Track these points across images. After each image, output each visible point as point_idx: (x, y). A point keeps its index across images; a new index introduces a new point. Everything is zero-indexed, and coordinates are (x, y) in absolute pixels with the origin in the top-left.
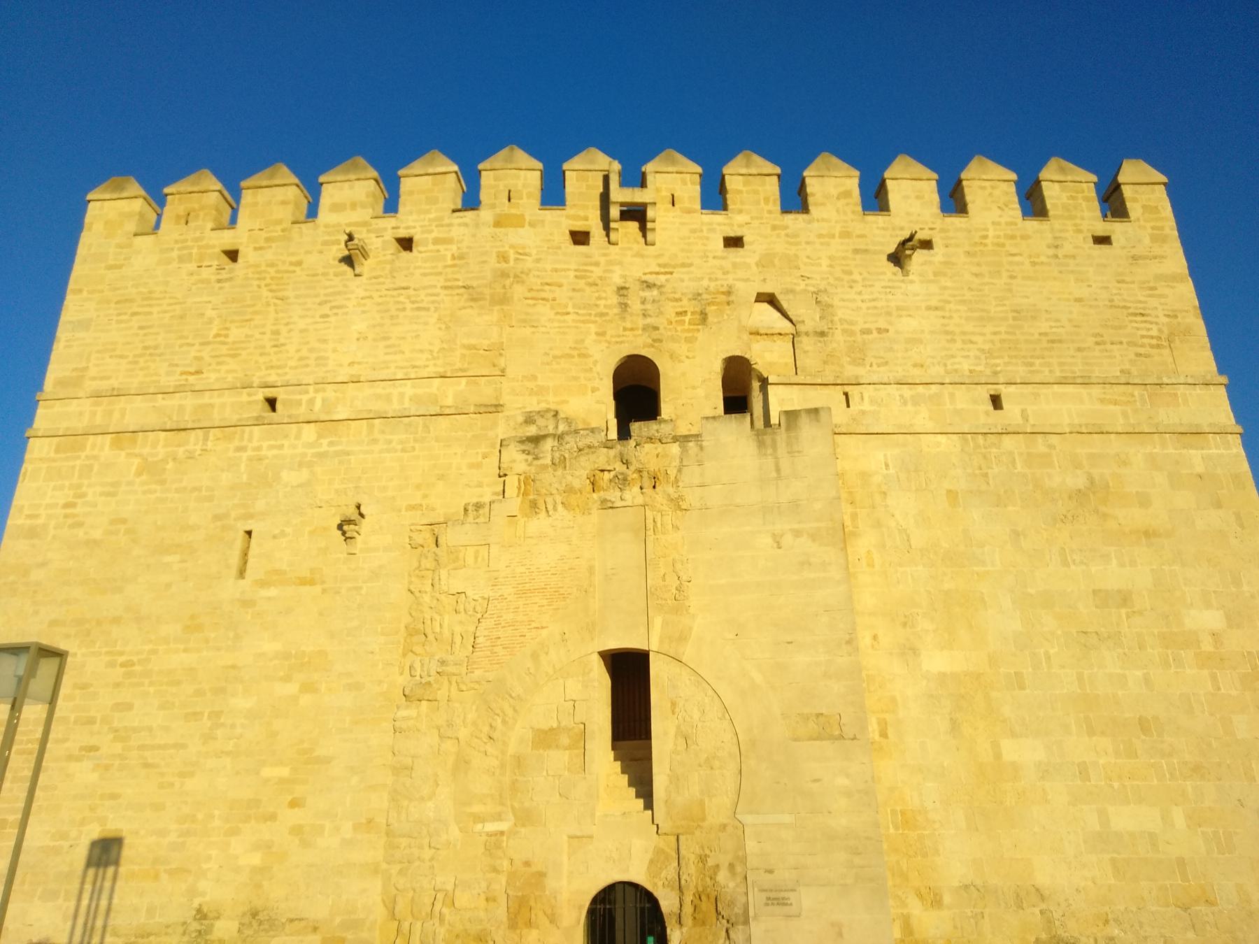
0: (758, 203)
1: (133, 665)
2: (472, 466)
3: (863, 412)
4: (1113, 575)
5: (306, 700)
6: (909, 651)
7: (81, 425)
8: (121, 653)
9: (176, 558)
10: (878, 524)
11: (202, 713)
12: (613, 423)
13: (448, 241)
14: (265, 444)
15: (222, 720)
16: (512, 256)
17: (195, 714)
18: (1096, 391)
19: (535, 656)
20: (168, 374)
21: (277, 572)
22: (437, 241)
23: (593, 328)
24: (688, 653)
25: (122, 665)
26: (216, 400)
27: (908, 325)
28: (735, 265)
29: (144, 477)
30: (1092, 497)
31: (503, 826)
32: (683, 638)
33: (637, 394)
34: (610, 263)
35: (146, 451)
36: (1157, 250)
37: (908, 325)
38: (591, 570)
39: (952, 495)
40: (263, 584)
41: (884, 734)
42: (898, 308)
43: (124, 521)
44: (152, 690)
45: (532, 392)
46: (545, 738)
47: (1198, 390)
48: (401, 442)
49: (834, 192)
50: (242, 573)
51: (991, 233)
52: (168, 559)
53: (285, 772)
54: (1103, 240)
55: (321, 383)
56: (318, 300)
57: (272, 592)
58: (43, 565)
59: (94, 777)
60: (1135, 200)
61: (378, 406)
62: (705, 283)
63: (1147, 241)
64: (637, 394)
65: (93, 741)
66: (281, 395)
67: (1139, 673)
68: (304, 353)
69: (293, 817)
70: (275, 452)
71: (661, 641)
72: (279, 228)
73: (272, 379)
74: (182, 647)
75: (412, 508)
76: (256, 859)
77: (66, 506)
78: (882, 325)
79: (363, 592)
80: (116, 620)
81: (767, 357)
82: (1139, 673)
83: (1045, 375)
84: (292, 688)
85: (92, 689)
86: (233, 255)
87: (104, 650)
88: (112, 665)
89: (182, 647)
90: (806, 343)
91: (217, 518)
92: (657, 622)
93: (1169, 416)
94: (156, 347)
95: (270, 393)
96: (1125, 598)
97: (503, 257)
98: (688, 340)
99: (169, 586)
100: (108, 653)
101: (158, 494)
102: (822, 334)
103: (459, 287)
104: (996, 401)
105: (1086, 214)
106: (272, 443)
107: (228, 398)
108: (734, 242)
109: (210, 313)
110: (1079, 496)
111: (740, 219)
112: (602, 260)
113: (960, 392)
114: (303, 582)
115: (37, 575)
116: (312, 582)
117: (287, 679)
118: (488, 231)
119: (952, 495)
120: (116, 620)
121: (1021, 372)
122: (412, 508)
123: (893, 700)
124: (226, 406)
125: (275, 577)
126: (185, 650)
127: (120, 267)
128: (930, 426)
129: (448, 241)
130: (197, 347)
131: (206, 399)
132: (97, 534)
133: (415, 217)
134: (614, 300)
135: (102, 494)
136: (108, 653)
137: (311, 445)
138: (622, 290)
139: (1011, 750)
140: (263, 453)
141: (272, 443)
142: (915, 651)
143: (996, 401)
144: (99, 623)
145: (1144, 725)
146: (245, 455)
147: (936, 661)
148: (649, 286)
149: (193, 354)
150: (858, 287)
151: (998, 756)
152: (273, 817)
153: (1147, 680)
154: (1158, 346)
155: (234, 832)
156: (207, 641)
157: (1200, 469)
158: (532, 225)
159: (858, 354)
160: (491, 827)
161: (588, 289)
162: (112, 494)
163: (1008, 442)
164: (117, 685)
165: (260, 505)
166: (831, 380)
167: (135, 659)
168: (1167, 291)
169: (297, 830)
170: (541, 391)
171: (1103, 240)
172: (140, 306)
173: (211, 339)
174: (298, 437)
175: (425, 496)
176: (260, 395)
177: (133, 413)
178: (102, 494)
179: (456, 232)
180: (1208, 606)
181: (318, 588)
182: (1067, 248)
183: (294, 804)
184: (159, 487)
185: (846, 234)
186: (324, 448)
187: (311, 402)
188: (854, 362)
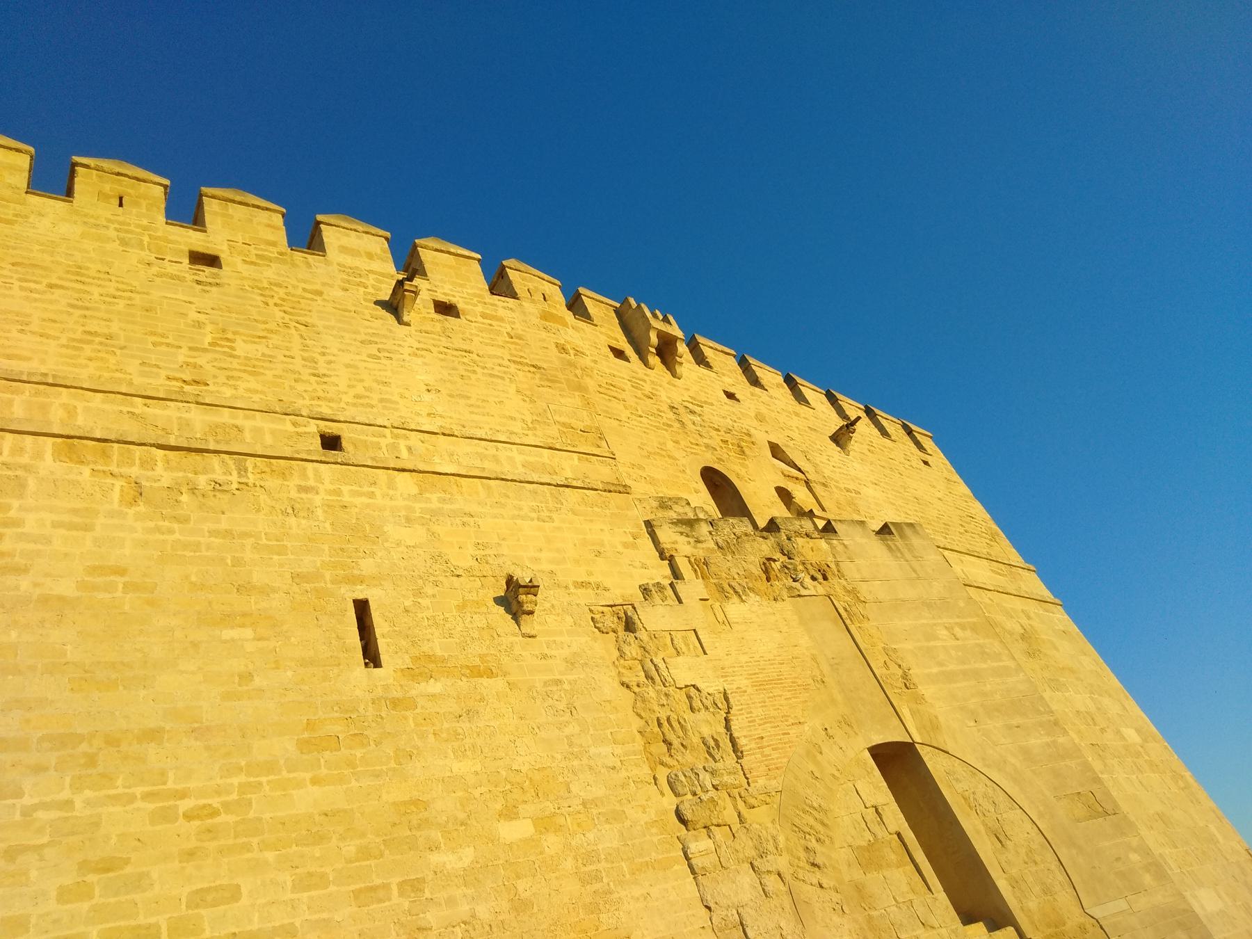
1: (215, 813)
2: (626, 545)
5: (552, 843)
8: (183, 795)
9: (248, 633)
11: (386, 887)
15: (427, 894)
17: (373, 889)
21: (430, 658)
25: (188, 817)
26: (240, 419)
29: (142, 508)
35: (135, 471)
43: (121, 572)
44: (270, 856)
46: (868, 857)
52: (228, 634)
56: (359, 338)
57: (434, 687)
61: (490, 467)
68: (360, 389)
70: (365, 500)
71: (920, 734)
72: (275, 250)
73: (326, 410)
74: (308, 776)
79: (566, 686)
80: (153, 735)
85: (128, 870)
87: (139, 791)
88: (166, 816)
89: (308, 776)
91: (297, 577)
95: (332, 428)
99: (246, 677)
100: (147, 796)
101: (177, 536)
103: (527, 364)
106: (355, 488)
107: (260, 421)
114: (476, 672)
116: (490, 674)
117: (510, 813)
120: (153, 735)
124: (265, 433)
125: (425, 666)
126: (315, 781)
130: (184, 351)
131: (225, 416)
132: (66, 588)
135: (55, 525)
136: (147, 796)
140: (347, 498)
141: (355, 488)
144: (112, 741)
146: (318, 500)
149: (181, 359)
156: (351, 764)
162: (87, 528)
164: (191, 854)
167: (215, 802)
172: (60, 278)
173: (206, 346)
174: (391, 485)
175: (590, 574)
176: (313, 427)
177: (92, 415)
178: (55, 525)
181: (499, 684)
184: (176, 526)
186: (435, 505)
187: (394, 447)
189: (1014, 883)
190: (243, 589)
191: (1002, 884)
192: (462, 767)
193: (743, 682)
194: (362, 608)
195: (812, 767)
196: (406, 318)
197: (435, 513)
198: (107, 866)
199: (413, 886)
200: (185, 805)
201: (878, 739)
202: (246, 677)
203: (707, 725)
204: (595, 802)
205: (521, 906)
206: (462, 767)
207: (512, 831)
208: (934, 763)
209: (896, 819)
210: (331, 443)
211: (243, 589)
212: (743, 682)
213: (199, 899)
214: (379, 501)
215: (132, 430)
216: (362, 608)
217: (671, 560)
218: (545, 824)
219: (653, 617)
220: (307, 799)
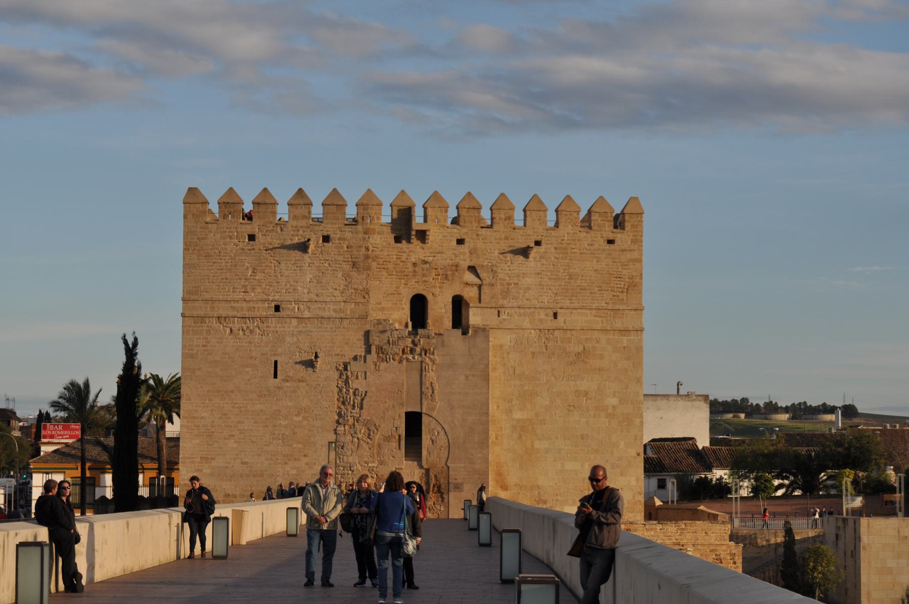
0: (471, 222)
3: (504, 320)
4: (584, 385)
5: (305, 422)
6: (509, 411)
7: (202, 313)
10: (504, 365)
12: (410, 324)
13: (344, 239)
16: (371, 248)
18: (594, 312)
19: (384, 412)
20: (234, 292)
22: (340, 239)
23: (403, 281)
24: (434, 414)
27: (529, 281)
28: (460, 253)
30: (582, 356)
31: (375, 465)
32: (433, 409)
33: (419, 307)
34: (411, 251)
35: (231, 325)
36: (632, 247)
37: (529, 281)
38: (403, 384)
39: (533, 353)
40: (286, 381)
41: (497, 438)
42: (524, 274)
45: (380, 310)
46: (388, 439)
47: (633, 312)
49: (503, 216)
50: (275, 376)
51: (566, 238)
52: (247, 369)
53: (301, 446)
54: (611, 242)
55: (297, 302)
57: (288, 384)
58: (199, 369)
59: (235, 445)
60: (629, 221)
62: (448, 261)
63: (629, 242)
64: (419, 307)
65: (233, 433)
66: (283, 306)
67: (585, 420)
69: (305, 460)
73: (277, 298)
75: (336, 355)
76: (294, 472)
77: (203, 346)
78: (515, 281)
80: (233, 391)
81: (470, 294)
82: (585, 420)
83: (576, 305)
84: (300, 418)
86: (252, 238)
88: (233, 407)
90: (485, 289)
92: (425, 403)
93: (618, 324)
96: (586, 394)
97: (367, 249)
98: (440, 287)
99: (249, 380)
102: (492, 285)
104: (555, 315)
105: (607, 229)
108: (460, 242)
109: (247, 264)
110: (578, 355)
111: (465, 230)
112: (407, 250)
113: (542, 312)
115: (198, 373)
117: (298, 414)
118: (361, 235)
119: (533, 353)
120: (233, 391)
121: (567, 303)
122: (336, 355)
123: (501, 428)
127: (204, 239)
128: (529, 326)
129: (344, 239)
132: (218, 358)
133: (329, 226)
134: (411, 269)
137: (296, 327)
138: (414, 264)
139: (537, 445)
142: (511, 411)
143: (555, 315)
145: (582, 437)
147: (518, 415)
148: (425, 262)
150: (509, 263)
151: (533, 446)
152: (299, 459)
153: (587, 422)
154: (622, 292)
155: (285, 463)
157: (625, 345)
158: (379, 233)
159: (506, 294)
160: (370, 465)
161: (401, 264)
163: (557, 333)
165: (280, 350)
166: (494, 305)
168: (631, 266)
169: (307, 464)
170: (383, 309)
171: (611, 242)
174: (290, 323)
179: (348, 235)
180: (614, 396)
181: (304, 384)
182: (596, 246)
183: (305, 456)
185: (507, 238)
188: (504, 298)
190: (251, 358)
192: (290, 404)
194: (276, 362)
197: (300, 332)
198: (225, 415)
201: (410, 410)
202: (249, 380)
204: (319, 415)
205: (294, 433)
206: (290, 404)
208: (425, 419)
210: (277, 308)
211: (251, 358)
212: (373, 389)
213: (238, 422)
214: (286, 329)
215: (231, 313)
216: (276, 362)
218: (305, 418)
219: (354, 367)
220: (258, 407)
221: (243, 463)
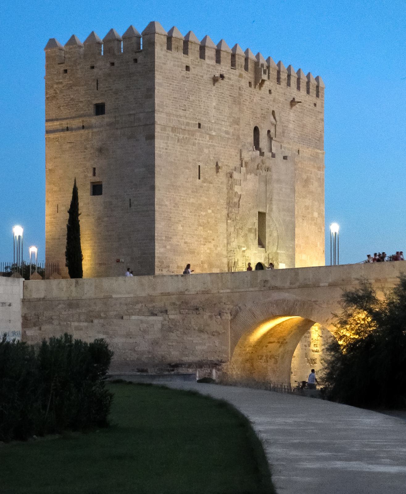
14: (200, 139)
46: (250, 230)
48: (224, 145)
57: (205, 184)
80: (179, 187)
94: (176, 98)
116: (212, 183)
189: (269, 243)
191: (267, 242)
193: (244, 193)
194: (199, 166)
195: (248, 213)
196: (216, 85)
199: (199, 216)
200: (182, 198)
203: (236, 200)
207: (210, 211)
208: (267, 217)
209: (256, 226)
216: (199, 166)
217: (242, 161)
219: (236, 175)
220: (192, 200)
221: (186, 243)
